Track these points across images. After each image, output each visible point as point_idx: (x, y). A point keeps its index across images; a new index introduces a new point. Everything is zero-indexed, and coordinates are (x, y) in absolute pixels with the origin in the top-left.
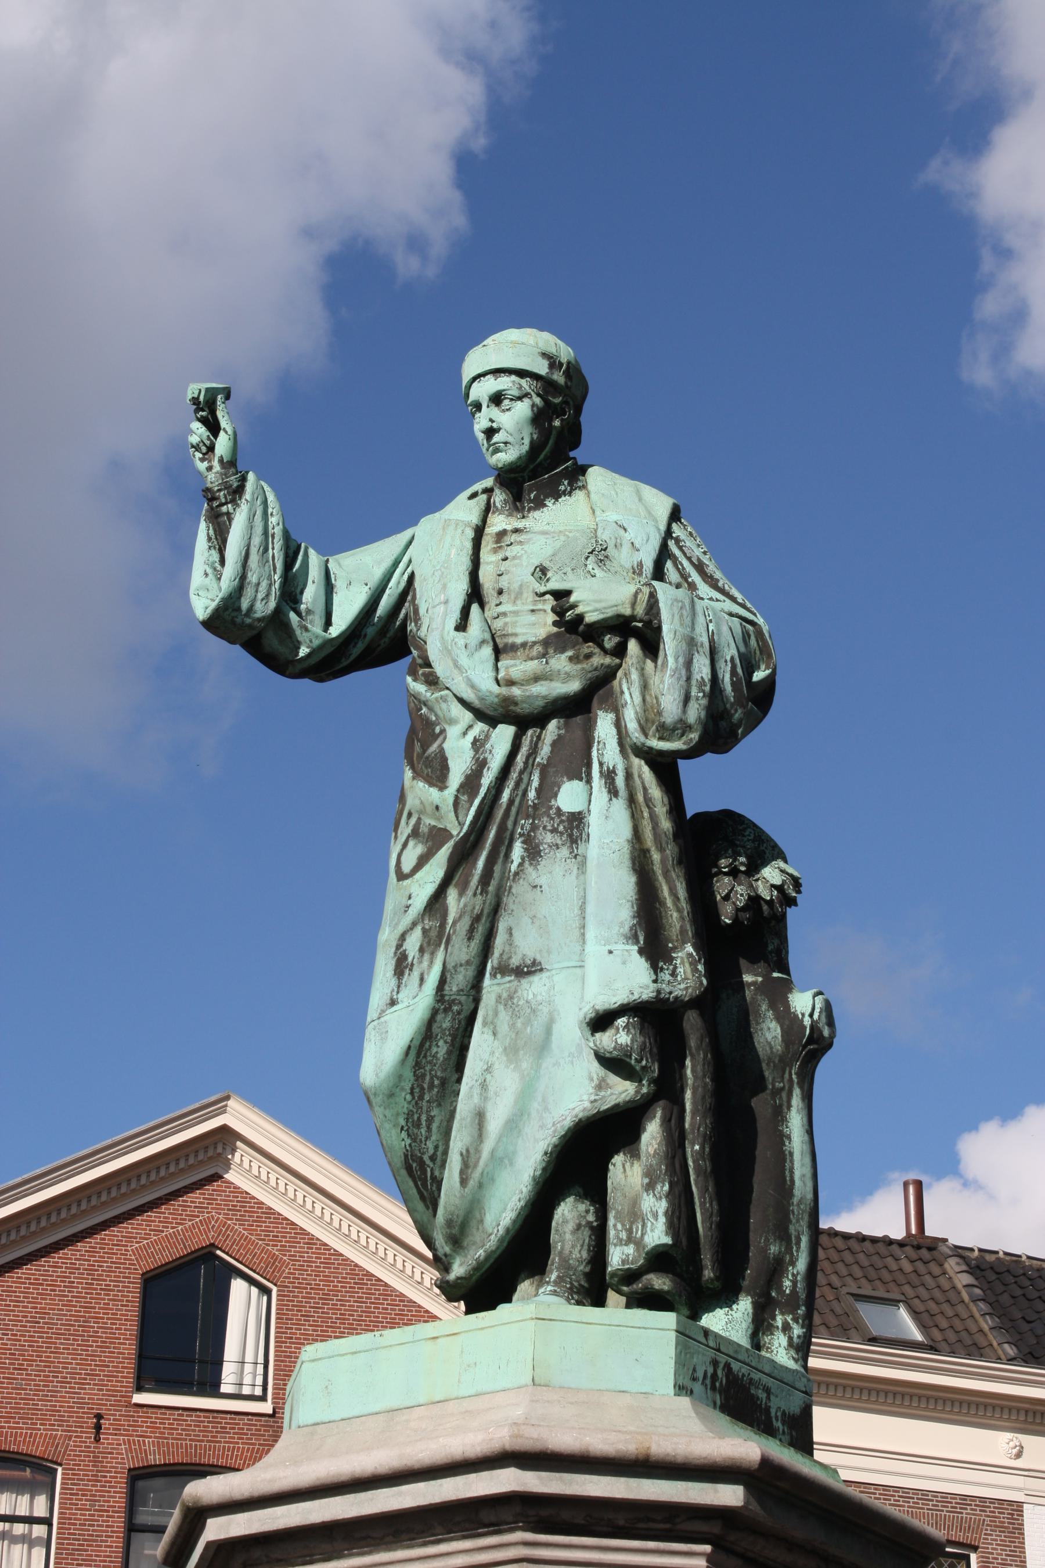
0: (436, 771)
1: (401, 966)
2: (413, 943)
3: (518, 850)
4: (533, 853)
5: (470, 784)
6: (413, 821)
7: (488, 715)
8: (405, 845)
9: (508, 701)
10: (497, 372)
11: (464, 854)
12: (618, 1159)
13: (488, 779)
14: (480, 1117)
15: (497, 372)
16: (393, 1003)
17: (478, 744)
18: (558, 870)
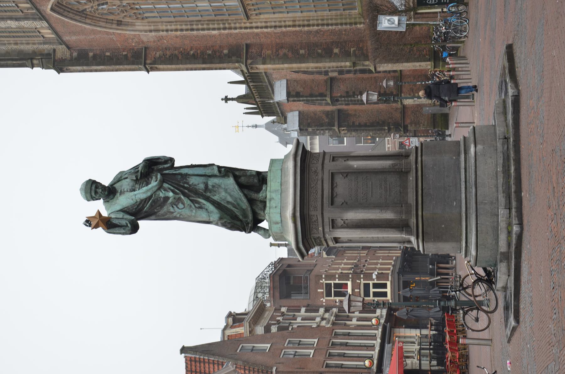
0: (167, 199)
1: (201, 208)
2: (197, 205)
3: (186, 185)
4: (188, 183)
5: (173, 191)
6: (174, 206)
7: (160, 187)
8: (178, 208)
9: (160, 181)
10: (91, 186)
11: (185, 194)
12: (240, 180)
13: (172, 188)
14: (228, 202)
15: (91, 186)
16: (207, 210)
17: (165, 190)
18: (190, 179)
